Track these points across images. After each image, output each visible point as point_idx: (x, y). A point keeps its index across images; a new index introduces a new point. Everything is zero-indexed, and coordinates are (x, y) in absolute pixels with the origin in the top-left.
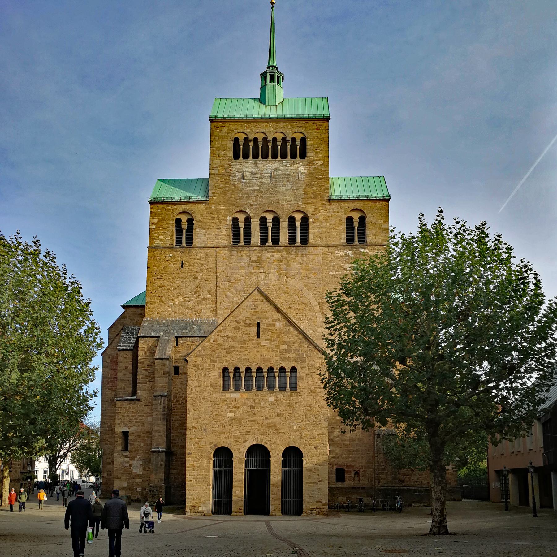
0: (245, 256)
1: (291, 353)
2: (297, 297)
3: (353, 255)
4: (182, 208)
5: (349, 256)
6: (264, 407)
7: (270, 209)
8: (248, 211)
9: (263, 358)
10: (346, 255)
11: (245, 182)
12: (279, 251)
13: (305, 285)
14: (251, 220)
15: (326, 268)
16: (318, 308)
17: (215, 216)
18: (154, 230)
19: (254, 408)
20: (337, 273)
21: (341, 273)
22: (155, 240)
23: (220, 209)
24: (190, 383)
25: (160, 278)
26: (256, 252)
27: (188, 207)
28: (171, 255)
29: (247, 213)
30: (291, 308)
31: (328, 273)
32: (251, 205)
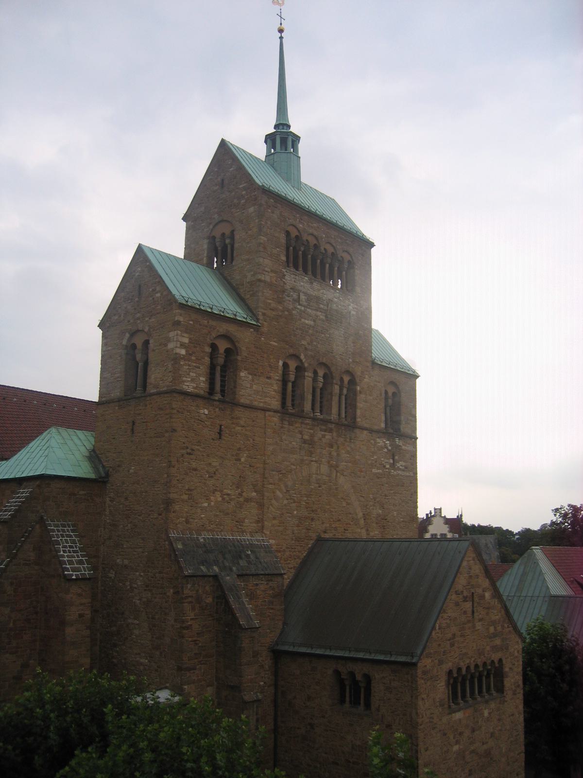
0: (297, 431)
1: (497, 638)
2: (344, 504)
3: (390, 448)
4: (224, 328)
5: (387, 448)
6: (481, 727)
7: (324, 361)
8: (302, 357)
9: (479, 650)
10: (386, 444)
11: (301, 310)
12: (331, 431)
13: (353, 487)
14: (306, 374)
15: (370, 462)
16: (362, 522)
17: (265, 355)
18: (183, 358)
19: (473, 731)
20: (379, 471)
21: (381, 471)
22: (184, 379)
23: (270, 345)
24: (420, 703)
25: (190, 454)
26: (308, 427)
27: (232, 329)
28: (206, 412)
29: (301, 361)
30: (339, 520)
31: (371, 471)
32: (306, 349)
